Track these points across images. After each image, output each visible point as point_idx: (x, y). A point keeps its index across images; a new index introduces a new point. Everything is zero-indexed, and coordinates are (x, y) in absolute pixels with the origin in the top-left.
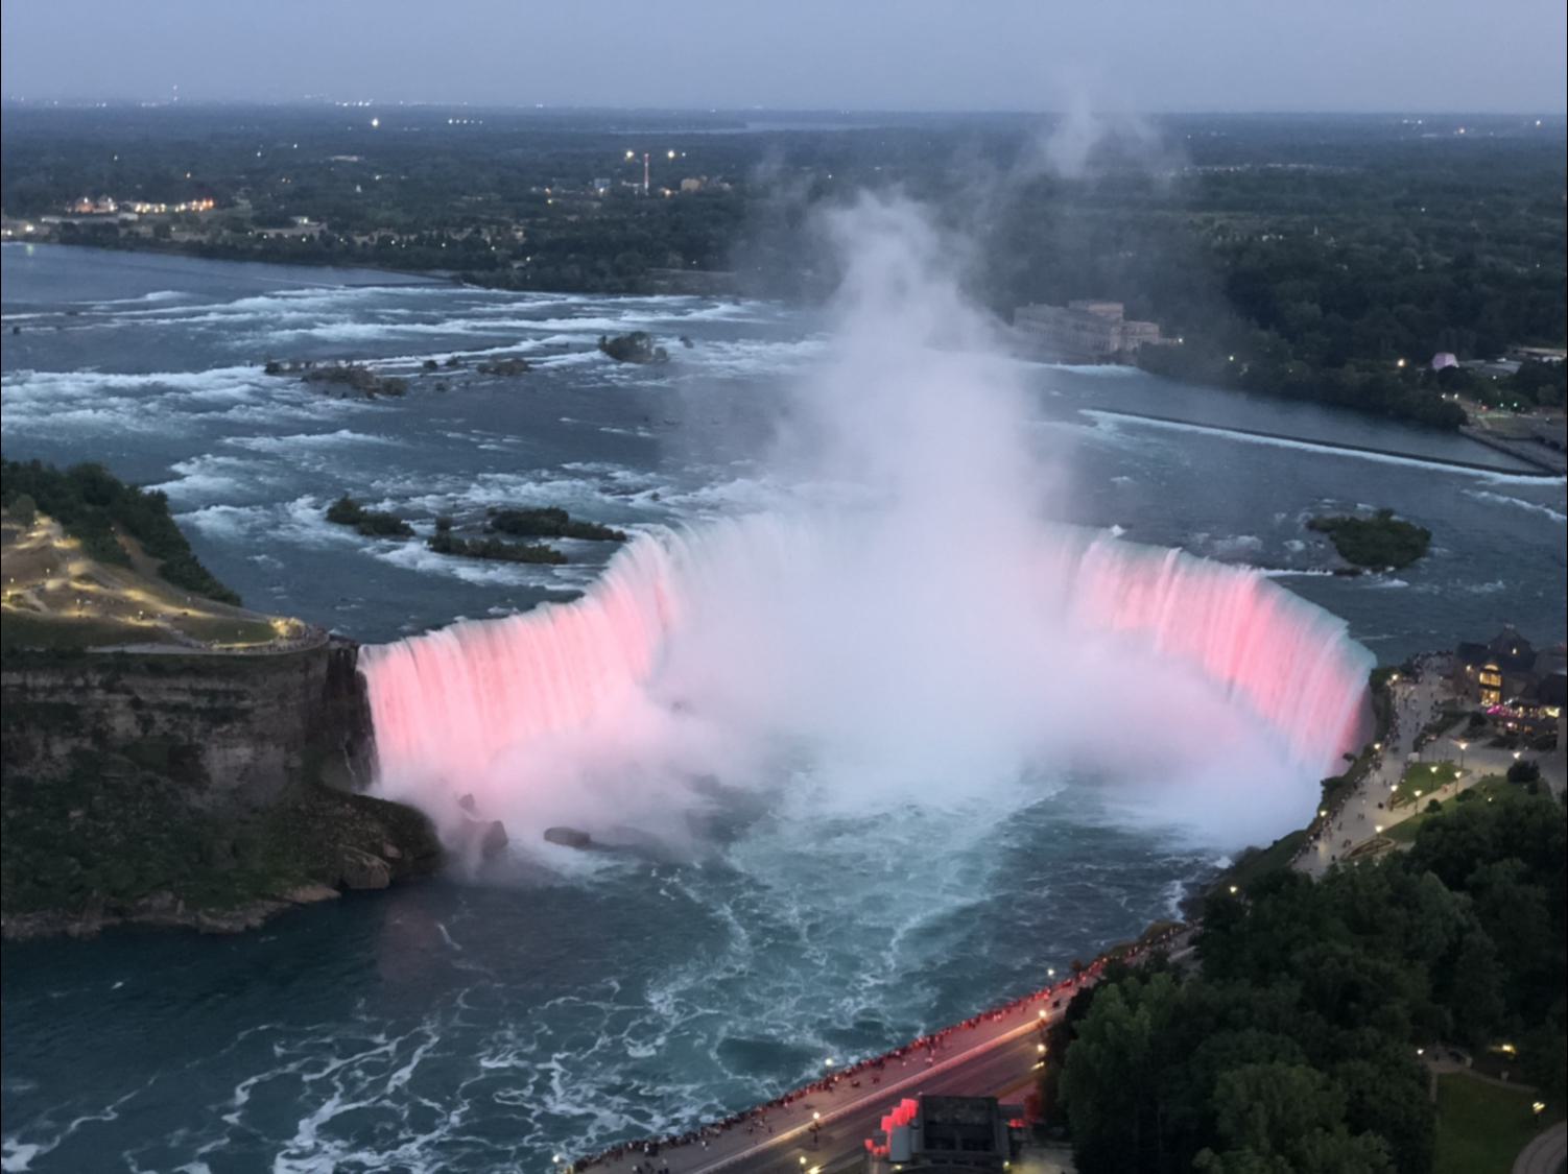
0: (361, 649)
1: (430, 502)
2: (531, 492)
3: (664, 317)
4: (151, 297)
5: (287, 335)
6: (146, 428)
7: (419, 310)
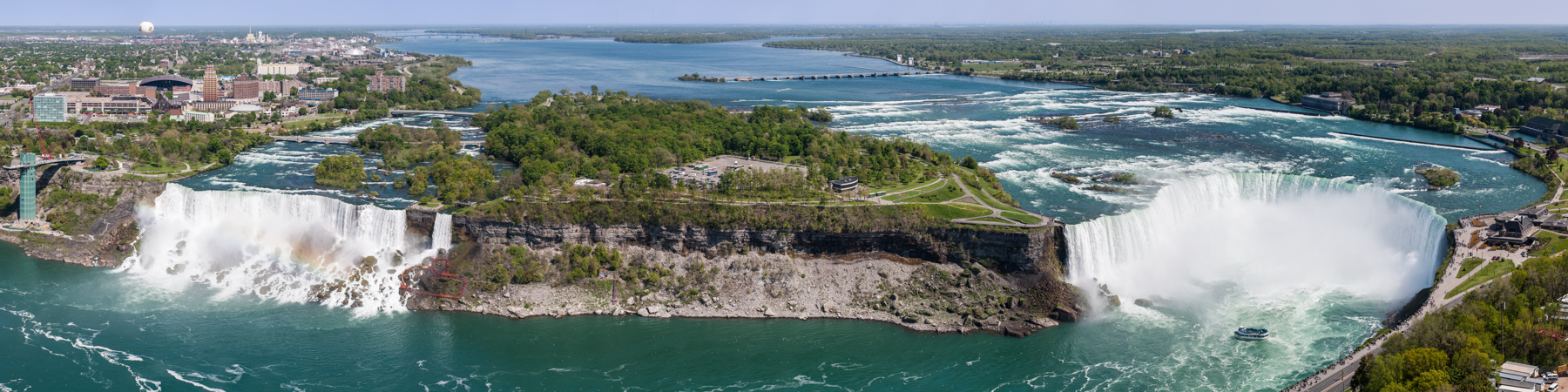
0: (1067, 226)
1: (1089, 170)
2: (1123, 166)
3: (1171, 100)
4: (986, 93)
5: (1033, 107)
6: (987, 141)
7: (1080, 98)
